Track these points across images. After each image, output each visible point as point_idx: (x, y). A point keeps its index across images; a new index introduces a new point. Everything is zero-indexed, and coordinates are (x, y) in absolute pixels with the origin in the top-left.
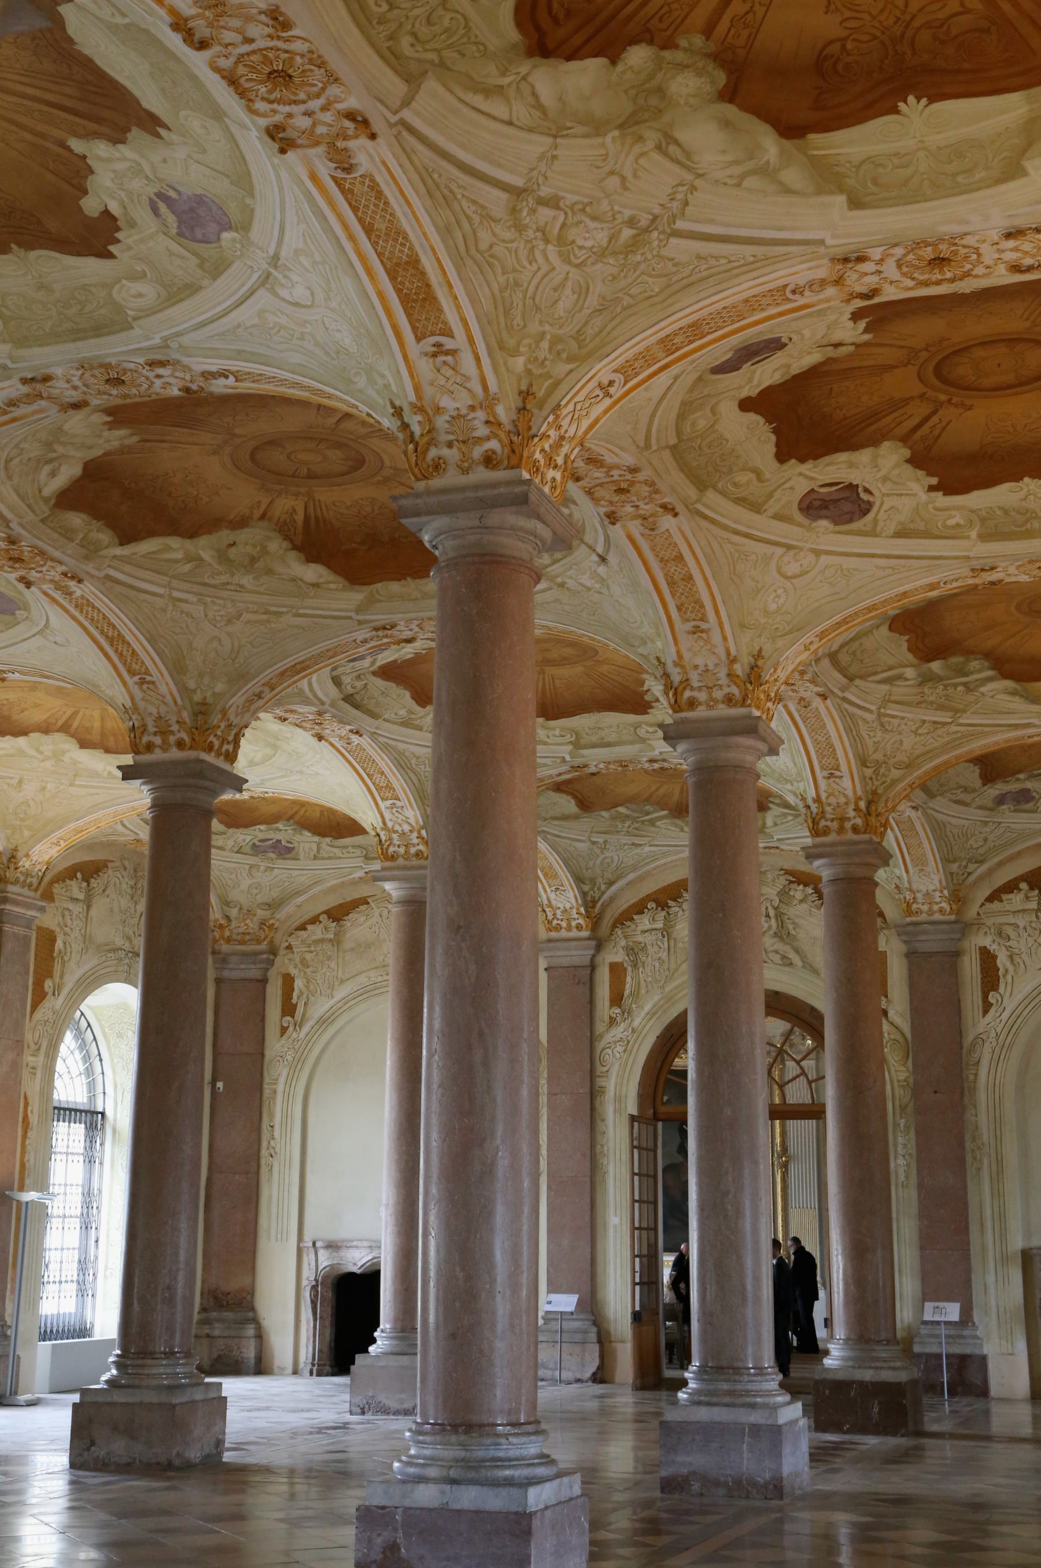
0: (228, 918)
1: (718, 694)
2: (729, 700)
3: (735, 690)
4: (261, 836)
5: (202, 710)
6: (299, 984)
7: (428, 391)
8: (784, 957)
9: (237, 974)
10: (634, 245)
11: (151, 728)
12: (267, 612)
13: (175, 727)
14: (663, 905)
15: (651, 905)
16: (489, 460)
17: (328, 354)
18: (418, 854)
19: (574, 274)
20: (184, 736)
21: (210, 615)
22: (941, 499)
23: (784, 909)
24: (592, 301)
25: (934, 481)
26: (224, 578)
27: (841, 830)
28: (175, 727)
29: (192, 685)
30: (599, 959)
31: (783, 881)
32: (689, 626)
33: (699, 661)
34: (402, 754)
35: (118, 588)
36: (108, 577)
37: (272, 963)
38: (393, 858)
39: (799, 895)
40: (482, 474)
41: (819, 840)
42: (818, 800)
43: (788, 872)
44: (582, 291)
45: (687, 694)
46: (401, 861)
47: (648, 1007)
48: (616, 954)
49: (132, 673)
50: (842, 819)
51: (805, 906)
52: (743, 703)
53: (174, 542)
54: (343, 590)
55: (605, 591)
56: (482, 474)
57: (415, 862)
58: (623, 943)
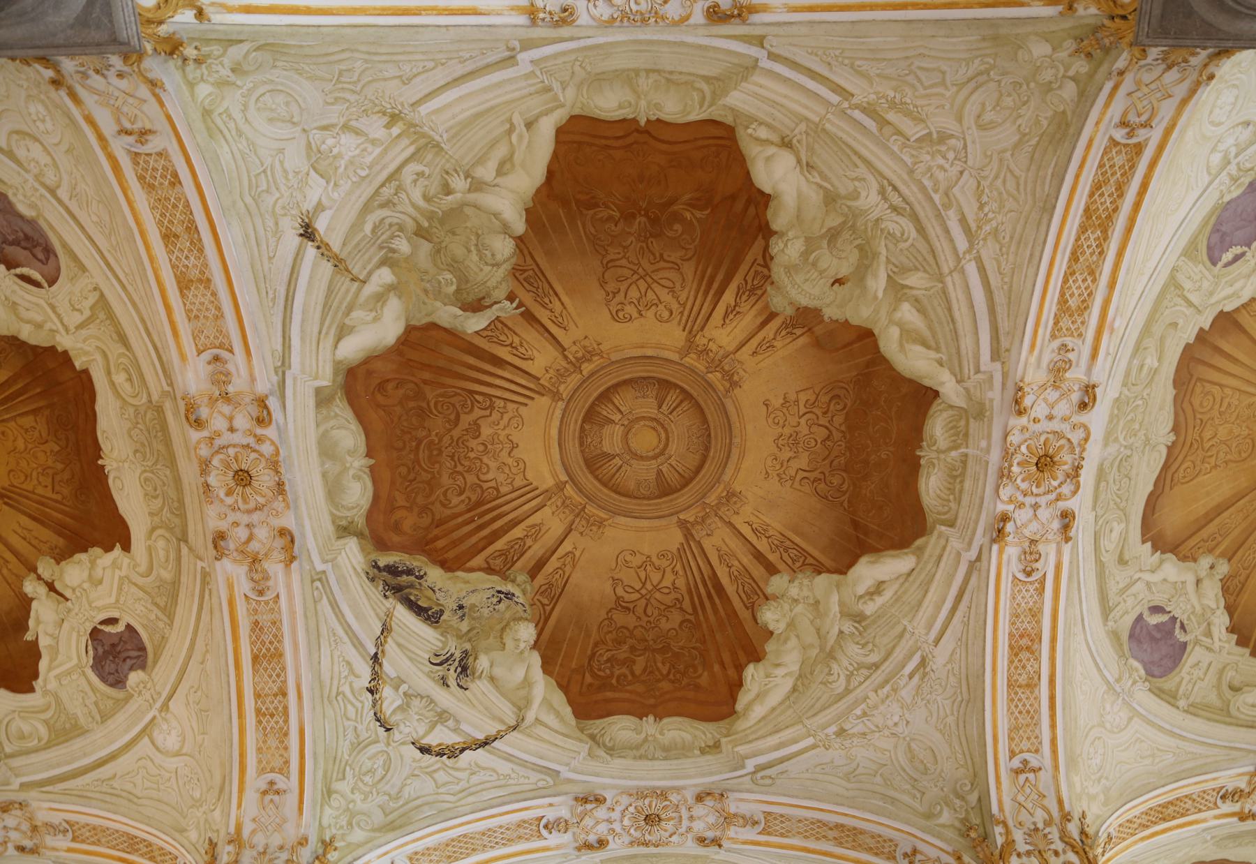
12: (883, 123)
21: (954, 171)
29: (1070, 90)
35: (1004, 325)
36: (996, 355)
49: (1139, 149)
53: (890, 343)
54: (752, 119)
55: (316, 136)
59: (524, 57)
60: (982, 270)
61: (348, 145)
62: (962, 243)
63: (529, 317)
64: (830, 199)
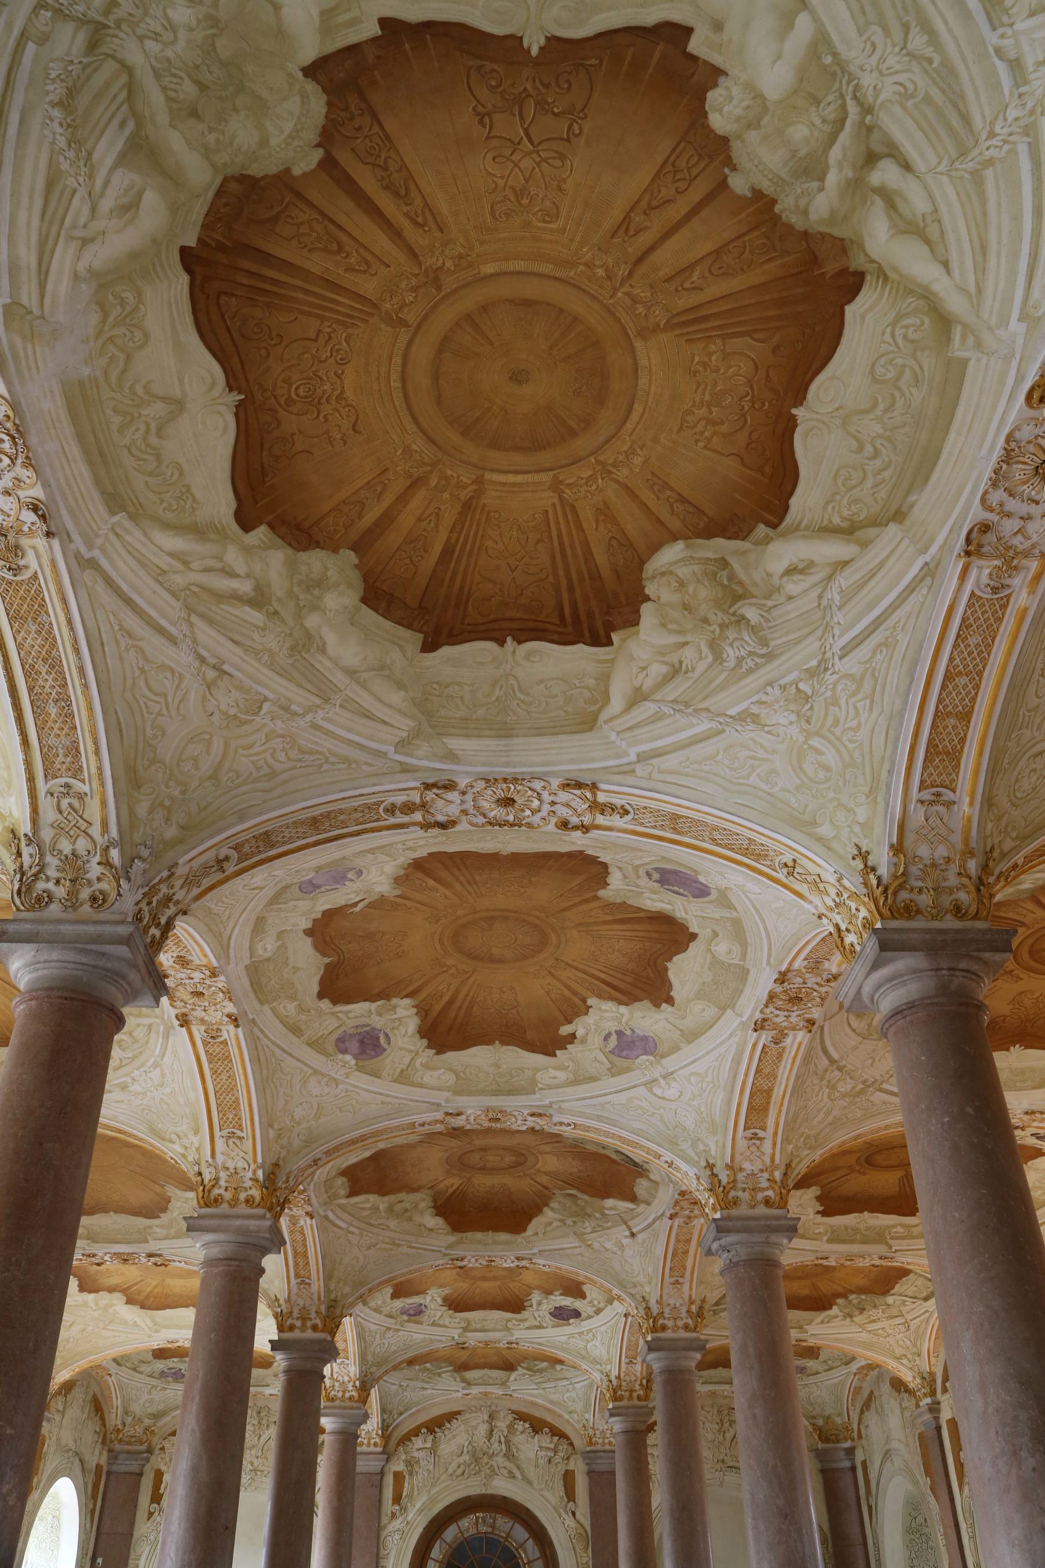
0: (124, 1424)
1: (680, 1323)
2: (686, 1327)
3: (690, 1321)
4: (171, 1365)
5: (332, 1305)
6: (166, 1478)
7: (738, 1158)
8: (510, 1472)
9: (122, 1468)
10: (861, 1092)
11: (295, 1315)
12: (394, 1244)
13: (313, 1315)
14: (431, 1431)
15: (424, 1430)
16: (767, 1202)
17: (666, 1126)
18: (351, 1398)
19: (829, 1104)
20: (318, 1322)
22: (820, 1219)
23: (511, 1437)
24: (830, 1119)
25: (821, 1208)
26: (380, 1221)
27: (631, 1398)
28: (313, 1315)
30: (386, 1469)
31: (510, 1417)
32: (673, 1280)
33: (672, 1302)
34: (363, 1329)
35: (327, 1223)
36: (326, 1217)
37: (148, 1460)
38: (333, 1400)
39: (520, 1428)
40: (762, 1210)
41: (617, 1404)
42: (618, 1377)
43: (513, 1412)
44: (828, 1113)
45: (661, 1321)
46: (338, 1403)
47: (418, 1506)
48: (398, 1465)
49: (297, 1276)
50: (632, 1391)
51: (524, 1436)
52: (695, 1330)
53: (373, 1198)
56: (762, 1210)
57: (348, 1404)
58: (404, 1457)
59: (535, 1250)
60: (340, 1228)
61: (608, 1245)
62: (351, 1229)
63: (546, 1188)
64: (410, 1219)
